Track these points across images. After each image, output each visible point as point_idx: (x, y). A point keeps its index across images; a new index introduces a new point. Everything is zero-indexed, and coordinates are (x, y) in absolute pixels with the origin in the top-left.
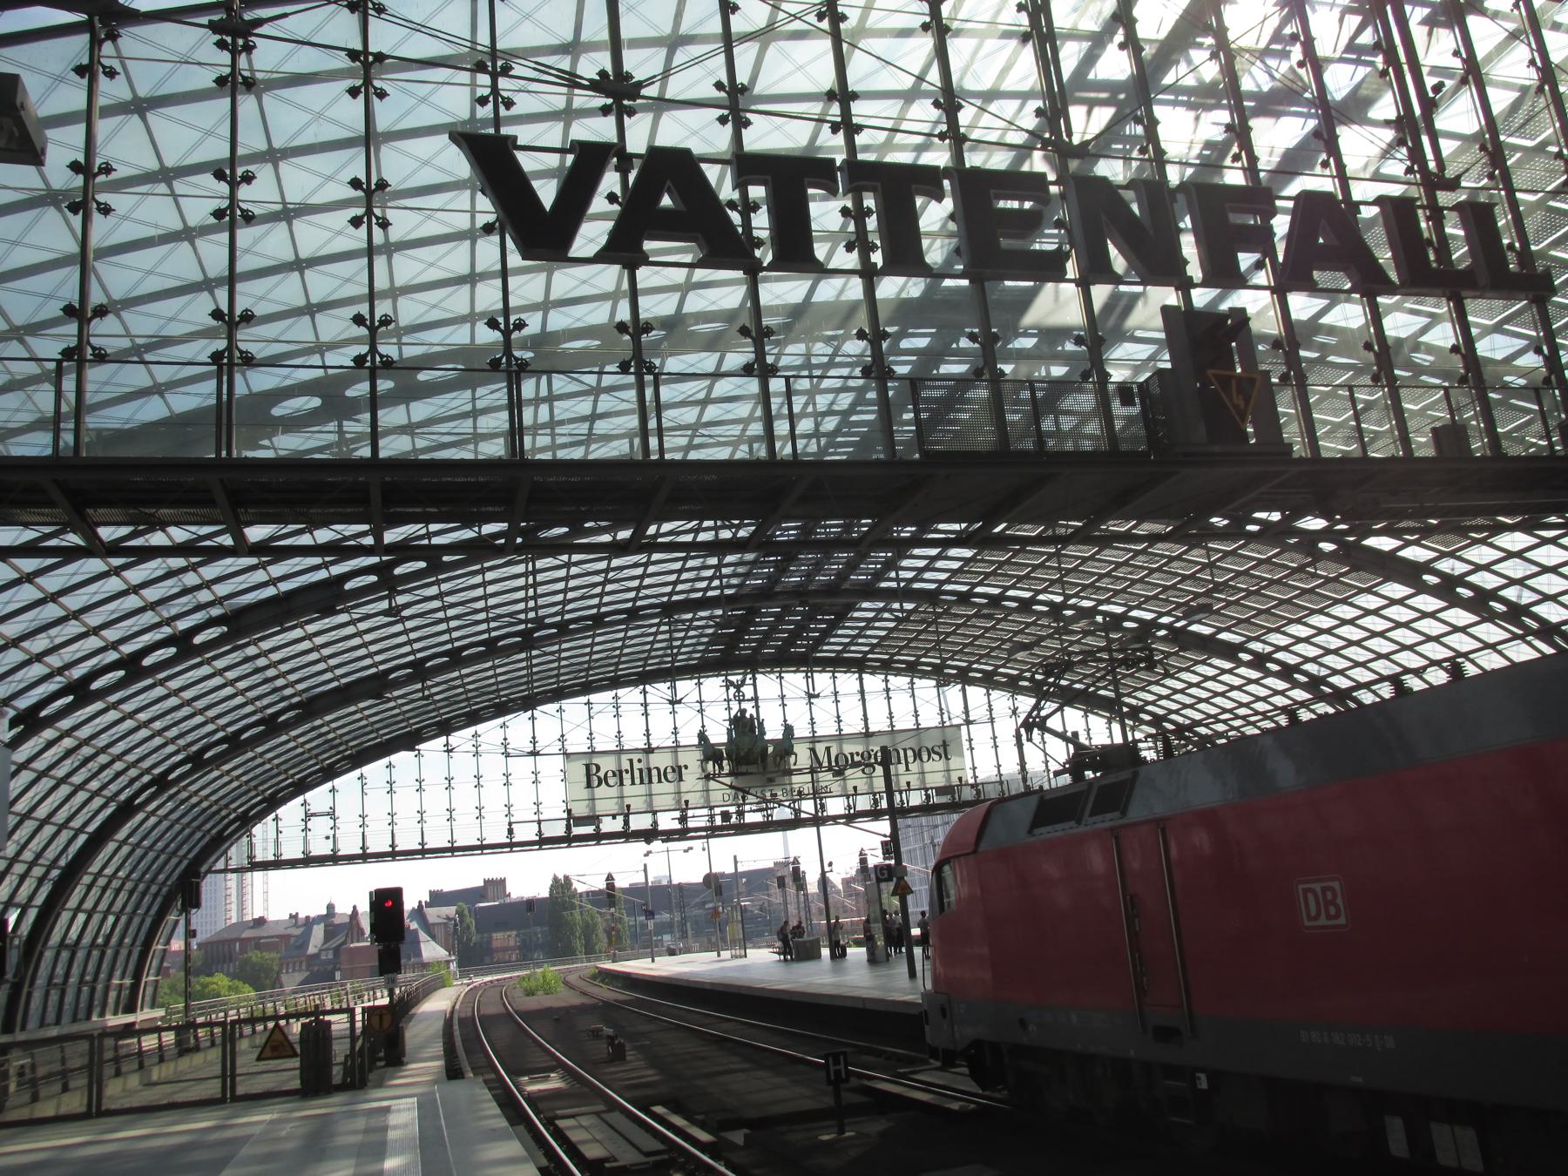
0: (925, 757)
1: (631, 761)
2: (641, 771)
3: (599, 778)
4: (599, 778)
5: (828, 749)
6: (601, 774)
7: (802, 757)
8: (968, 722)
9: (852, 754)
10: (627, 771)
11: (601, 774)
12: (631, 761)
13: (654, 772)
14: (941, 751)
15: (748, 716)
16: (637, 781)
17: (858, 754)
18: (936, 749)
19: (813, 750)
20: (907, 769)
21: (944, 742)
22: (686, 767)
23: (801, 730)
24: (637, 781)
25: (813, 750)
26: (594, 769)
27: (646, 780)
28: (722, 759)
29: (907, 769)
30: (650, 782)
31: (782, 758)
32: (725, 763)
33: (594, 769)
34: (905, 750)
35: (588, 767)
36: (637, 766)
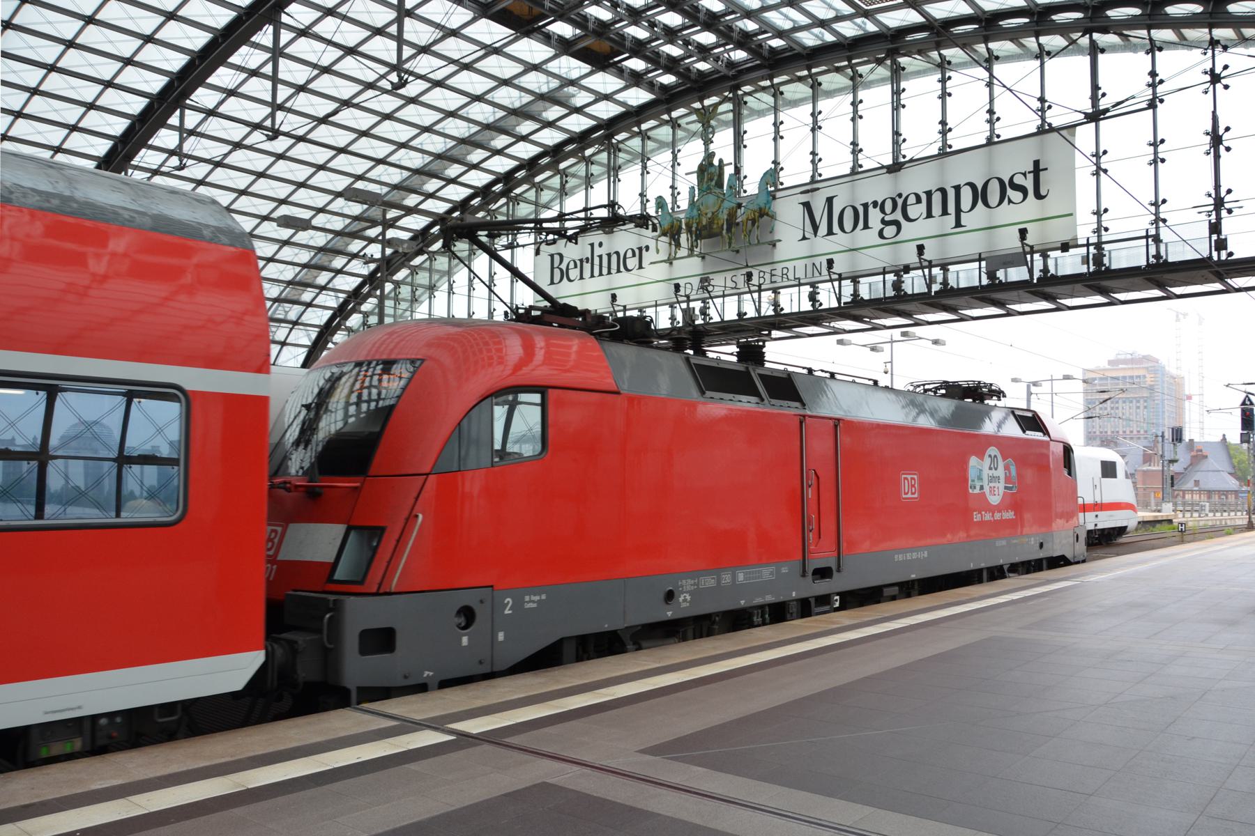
0: (994, 196)
1: (592, 245)
2: (600, 257)
3: (561, 270)
4: (561, 270)
5: (830, 201)
6: (564, 266)
7: (789, 213)
8: (1095, 116)
9: (866, 206)
10: (587, 259)
11: (564, 266)
12: (592, 245)
13: (614, 258)
14: (1029, 183)
15: (716, 162)
16: (596, 272)
17: (875, 204)
18: (1019, 180)
19: (807, 205)
20: (958, 224)
21: (1036, 163)
22: (647, 248)
23: (795, 173)
24: (596, 272)
25: (807, 205)
26: (557, 258)
27: (605, 271)
28: (679, 233)
29: (958, 224)
30: (609, 273)
31: (753, 224)
32: (684, 238)
33: (557, 258)
34: (957, 189)
35: (552, 256)
36: (598, 251)
